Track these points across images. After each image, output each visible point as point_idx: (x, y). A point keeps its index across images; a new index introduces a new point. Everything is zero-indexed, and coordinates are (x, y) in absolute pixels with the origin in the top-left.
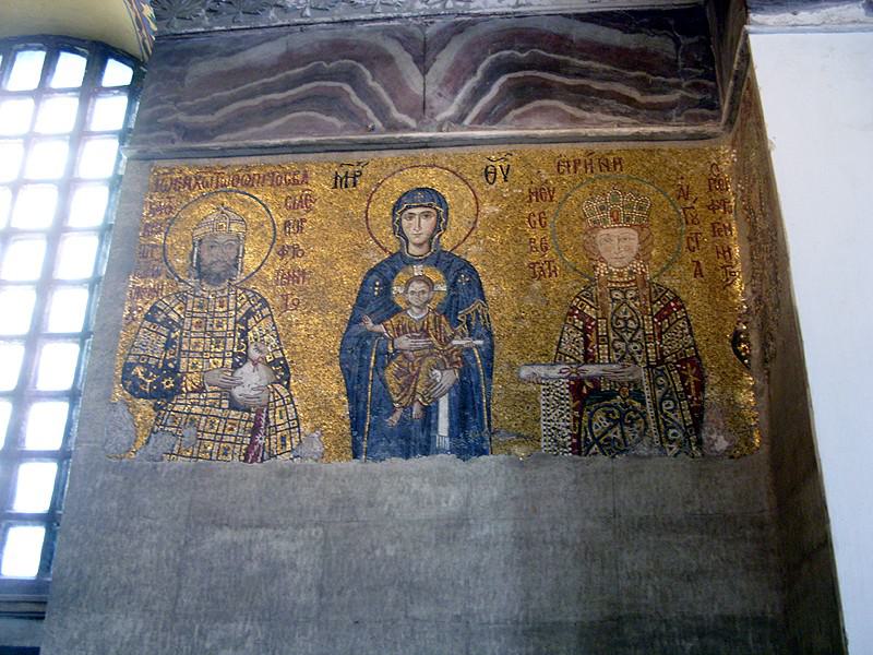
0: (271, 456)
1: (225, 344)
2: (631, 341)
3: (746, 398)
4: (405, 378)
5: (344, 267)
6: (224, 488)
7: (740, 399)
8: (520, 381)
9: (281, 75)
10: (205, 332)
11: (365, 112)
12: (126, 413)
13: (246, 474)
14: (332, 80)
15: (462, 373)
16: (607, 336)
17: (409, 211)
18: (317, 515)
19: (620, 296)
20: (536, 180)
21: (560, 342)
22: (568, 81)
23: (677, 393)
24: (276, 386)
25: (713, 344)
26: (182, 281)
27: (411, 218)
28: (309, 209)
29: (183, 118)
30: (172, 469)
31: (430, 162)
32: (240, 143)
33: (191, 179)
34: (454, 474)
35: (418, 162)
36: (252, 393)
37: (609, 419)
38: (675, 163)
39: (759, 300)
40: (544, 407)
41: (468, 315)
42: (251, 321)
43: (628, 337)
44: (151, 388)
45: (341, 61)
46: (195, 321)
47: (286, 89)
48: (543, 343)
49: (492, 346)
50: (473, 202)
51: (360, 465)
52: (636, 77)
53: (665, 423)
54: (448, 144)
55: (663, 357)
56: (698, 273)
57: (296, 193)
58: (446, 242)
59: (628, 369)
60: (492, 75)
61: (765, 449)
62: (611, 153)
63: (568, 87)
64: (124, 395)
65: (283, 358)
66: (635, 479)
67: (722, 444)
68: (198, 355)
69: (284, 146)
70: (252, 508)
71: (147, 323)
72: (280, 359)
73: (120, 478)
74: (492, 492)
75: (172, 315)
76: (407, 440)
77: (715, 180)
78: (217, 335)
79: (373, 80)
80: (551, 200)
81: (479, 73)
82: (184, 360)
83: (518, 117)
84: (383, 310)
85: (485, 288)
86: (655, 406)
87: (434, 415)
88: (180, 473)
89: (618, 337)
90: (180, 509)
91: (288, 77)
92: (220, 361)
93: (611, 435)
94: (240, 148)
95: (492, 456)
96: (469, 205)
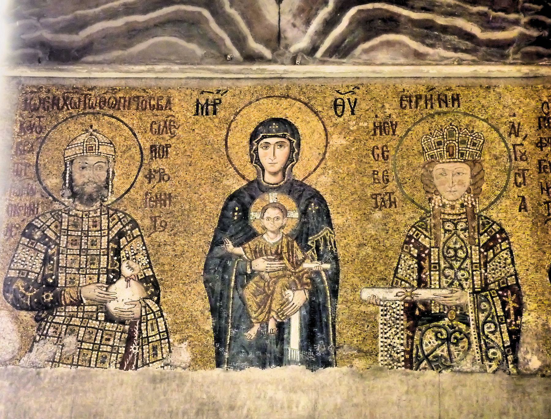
1: (100, 261)
2: (460, 269)
4: (261, 297)
5: (206, 191)
6: (103, 391)
8: (362, 302)
10: (80, 250)
12: (9, 324)
13: (122, 381)
15: (311, 294)
16: (439, 264)
17: (265, 140)
18: (186, 417)
20: (380, 115)
23: (498, 317)
27: (266, 147)
28: (173, 135)
29: (47, 35)
30: (54, 375)
31: (284, 92)
33: (59, 99)
34: (303, 382)
35: (274, 91)
36: (126, 307)
37: (437, 338)
40: (381, 326)
41: (317, 241)
42: (123, 240)
43: (457, 265)
44: (31, 301)
46: (70, 239)
47: (145, 12)
49: (337, 273)
52: (479, 14)
53: (486, 343)
55: (487, 285)
56: (523, 208)
57: (160, 118)
58: (298, 173)
59: (454, 295)
62: (450, 89)
64: (7, 307)
65: (154, 276)
66: (458, 391)
67: (535, 363)
68: (74, 271)
71: (25, 240)
73: (7, 384)
75: (49, 233)
77: (545, 118)
78: (91, 252)
79: (231, 6)
80: (394, 134)
84: (241, 234)
85: (332, 216)
86: (478, 327)
87: (286, 331)
88: (62, 378)
89: (447, 265)
90: (63, 412)
93: (438, 352)
95: (335, 368)
96: (319, 138)
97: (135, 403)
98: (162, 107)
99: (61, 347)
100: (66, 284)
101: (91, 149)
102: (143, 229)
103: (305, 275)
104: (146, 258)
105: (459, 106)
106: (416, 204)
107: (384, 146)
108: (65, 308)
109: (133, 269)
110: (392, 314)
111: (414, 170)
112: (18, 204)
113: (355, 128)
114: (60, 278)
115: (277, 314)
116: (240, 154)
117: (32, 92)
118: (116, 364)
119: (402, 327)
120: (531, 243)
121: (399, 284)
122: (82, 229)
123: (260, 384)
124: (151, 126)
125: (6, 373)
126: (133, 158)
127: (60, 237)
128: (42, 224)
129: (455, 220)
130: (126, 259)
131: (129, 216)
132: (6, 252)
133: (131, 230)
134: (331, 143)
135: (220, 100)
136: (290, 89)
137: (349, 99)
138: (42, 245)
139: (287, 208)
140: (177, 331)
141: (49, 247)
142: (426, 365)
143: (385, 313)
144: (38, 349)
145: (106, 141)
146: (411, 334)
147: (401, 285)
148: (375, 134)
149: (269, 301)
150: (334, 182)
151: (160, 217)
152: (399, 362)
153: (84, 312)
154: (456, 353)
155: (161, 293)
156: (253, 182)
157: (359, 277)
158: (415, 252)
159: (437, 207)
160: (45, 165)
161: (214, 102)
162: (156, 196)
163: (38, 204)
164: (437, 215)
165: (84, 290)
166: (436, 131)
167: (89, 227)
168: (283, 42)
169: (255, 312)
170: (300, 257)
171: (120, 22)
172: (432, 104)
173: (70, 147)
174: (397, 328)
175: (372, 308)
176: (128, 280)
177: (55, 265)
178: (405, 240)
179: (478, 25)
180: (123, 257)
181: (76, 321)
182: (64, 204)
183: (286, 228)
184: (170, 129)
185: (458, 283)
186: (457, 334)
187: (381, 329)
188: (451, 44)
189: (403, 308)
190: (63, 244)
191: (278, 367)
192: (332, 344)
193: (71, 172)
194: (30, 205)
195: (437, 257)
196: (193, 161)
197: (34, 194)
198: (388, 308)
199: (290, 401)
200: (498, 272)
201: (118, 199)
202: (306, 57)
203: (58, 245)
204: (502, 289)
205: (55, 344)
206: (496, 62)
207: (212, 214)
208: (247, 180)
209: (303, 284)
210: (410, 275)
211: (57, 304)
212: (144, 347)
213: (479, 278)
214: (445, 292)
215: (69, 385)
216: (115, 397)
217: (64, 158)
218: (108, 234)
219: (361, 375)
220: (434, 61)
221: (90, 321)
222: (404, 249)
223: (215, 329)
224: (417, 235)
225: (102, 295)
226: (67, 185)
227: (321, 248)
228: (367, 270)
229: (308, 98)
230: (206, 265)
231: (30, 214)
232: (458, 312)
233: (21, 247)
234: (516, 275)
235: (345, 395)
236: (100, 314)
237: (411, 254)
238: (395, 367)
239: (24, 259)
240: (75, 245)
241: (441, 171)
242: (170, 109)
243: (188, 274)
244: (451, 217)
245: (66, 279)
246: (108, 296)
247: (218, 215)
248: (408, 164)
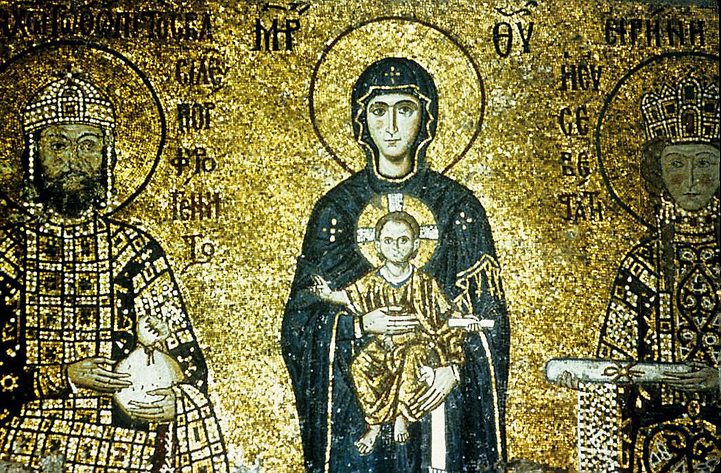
1: (97, 316)
2: (705, 329)
5: (280, 191)
8: (547, 383)
15: (463, 373)
16: (672, 321)
17: (378, 99)
21: (605, 326)
24: (185, 387)
36: (150, 399)
48: (581, 325)
50: (476, 86)
58: (437, 157)
62: (688, 12)
65: (195, 343)
72: (188, 345)
87: (425, 437)
92: (93, 346)
96: (470, 91)
100: (39, 359)
101: (70, 111)
102: (172, 259)
103: (453, 340)
104: (180, 310)
105: (702, 44)
107: (579, 109)
108: (41, 404)
109: (157, 331)
110: (599, 405)
114: (28, 348)
115: (408, 408)
119: (615, 428)
121: (609, 354)
122: (63, 257)
124: (178, 66)
126: (149, 129)
129: (696, 244)
130: (143, 312)
131: (148, 236)
133: (151, 260)
134: (490, 104)
135: (297, 22)
137: (519, 25)
139: (420, 223)
140: (239, 441)
143: (588, 402)
145: (98, 96)
148: (564, 87)
149: (394, 387)
150: (498, 175)
151: (200, 236)
153: (74, 409)
155: (211, 372)
157: (543, 342)
158: (634, 300)
159: (667, 222)
161: (288, 25)
162: (192, 198)
166: (666, 87)
167: (75, 256)
169: (374, 404)
170: (444, 307)
173: (33, 106)
175: (563, 395)
177: (19, 325)
178: (617, 278)
180: (139, 308)
181: (60, 426)
183: (418, 257)
184: (212, 77)
185: (702, 354)
186: (702, 440)
187: (582, 430)
189: (615, 395)
190: (31, 287)
193: (37, 154)
195: (669, 309)
198: (592, 394)
203: (23, 289)
207: (291, 232)
208: (350, 171)
209: (449, 356)
210: (626, 339)
214: (680, 368)
221: (87, 426)
222: (616, 294)
223: (304, 435)
224: (637, 268)
225: (109, 379)
226: (32, 178)
227: (478, 292)
228: (555, 327)
229: (449, 22)
232: (704, 404)
236: (103, 413)
240: (53, 288)
242: (210, 37)
243: (254, 339)
246: (115, 381)
247: (301, 233)
248: (619, 144)
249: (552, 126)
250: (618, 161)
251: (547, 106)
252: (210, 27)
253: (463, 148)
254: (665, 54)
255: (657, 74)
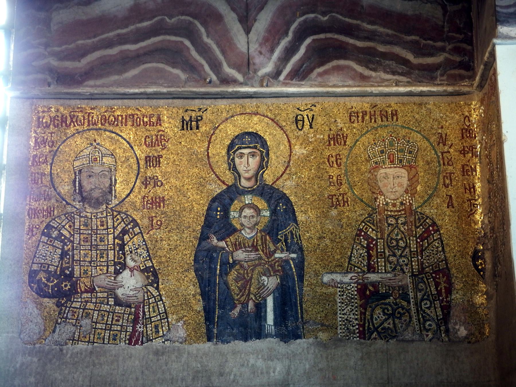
0: (149, 340)
1: (108, 255)
2: (401, 256)
3: (480, 299)
6: (116, 364)
7: (477, 301)
8: (323, 284)
9: (132, 27)
10: (91, 245)
11: (202, 66)
12: (35, 309)
13: (131, 354)
14: (176, 35)
16: (384, 252)
17: (240, 151)
18: (184, 383)
19: (393, 222)
20: (333, 128)
21: (351, 256)
22: (359, 44)
23: (432, 295)
25: (459, 259)
26: (70, 204)
28: (164, 148)
32: (106, 90)
35: (245, 109)
36: (131, 293)
37: (384, 314)
38: (437, 114)
39: (492, 229)
40: (339, 304)
41: (285, 235)
42: (126, 237)
43: (399, 253)
44: (52, 290)
45: (180, 17)
46: (82, 237)
47: (136, 42)
48: (339, 257)
51: (213, 347)
52: (412, 42)
53: (423, 317)
54: (269, 96)
55: (423, 269)
56: (450, 205)
58: (268, 177)
60: (299, 38)
61: (493, 337)
62: (390, 106)
63: (361, 50)
65: (153, 267)
66: (402, 356)
67: (463, 332)
68: (87, 264)
69: (141, 94)
70: (137, 379)
71: (44, 239)
73: (35, 359)
74: (304, 366)
75: (65, 232)
76: (245, 329)
77: (466, 130)
78: (101, 247)
79: (208, 36)
80: (345, 145)
81: (290, 34)
82: (77, 268)
83: (320, 75)
84: (223, 230)
85: (297, 214)
86: (416, 304)
87: (263, 310)
88: (81, 354)
89: (391, 253)
90: (83, 381)
91: (138, 30)
92: (105, 268)
93: (386, 325)
94: (105, 94)
95: (304, 340)
96: (284, 147)
97: (142, 372)
98: (153, 123)
99: (79, 327)
100: (80, 274)
106: (365, 203)
107: (337, 155)
108: (81, 295)
111: (362, 175)
112: (37, 208)
113: (313, 139)
114: (75, 270)
115: (255, 296)
116: (219, 163)
117: (43, 112)
118: (125, 341)
119: (356, 305)
120: (457, 234)
122: (92, 227)
123: (243, 355)
124: (145, 139)
125: (34, 351)
126: (131, 168)
127: (74, 235)
128: (58, 224)
129: (396, 216)
131: (131, 217)
132: (28, 249)
134: (294, 152)
136: (259, 107)
137: (307, 115)
138: (59, 243)
141: (65, 244)
142: (376, 335)
144: (60, 330)
146: (363, 311)
147: (354, 270)
151: (156, 217)
152: (354, 334)
154: (400, 325)
155: (160, 280)
156: (231, 186)
157: (320, 265)
159: (381, 205)
160: (57, 174)
161: (197, 118)
163: (54, 208)
164: (382, 212)
165: (95, 279)
167: (97, 227)
168: (251, 67)
170: (272, 248)
171: (114, 51)
172: (375, 118)
174: (352, 306)
175: (331, 290)
176: (132, 270)
179: (411, 51)
182: (75, 207)
183: (260, 224)
184: (161, 142)
186: (400, 310)
187: (340, 307)
188: (390, 68)
189: (356, 289)
190: (76, 242)
191: (258, 340)
192: (300, 320)
194: (47, 208)
195: (382, 247)
196: (182, 169)
197: (50, 199)
199: (268, 368)
200: (431, 259)
201: (120, 202)
202: (271, 79)
203: (73, 242)
204: (435, 272)
205: (74, 326)
206: (427, 83)
208: (227, 185)
209: (275, 271)
210: (361, 262)
211: (74, 291)
212: (148, 326)
213: (417, 263)
214: (389, 275)
215: (88, 359)
216: (125, 368)
217: (74, 168)
218: (114, 231)
219: (325, 344)
220: (376, 82)
221: (102, 305)
226: (77, 191)
227: (289, 241)
228: (326, 258)
230: (195, 256)
231: (48, 217)
232: (401, 292)
233: (41, 244)
234: (446, 260)
235: (312, 361)
236: (110, 299)
237: (361, 245)
238: (352, 338)
239: (45, 255)
240: (87, 241)
241: (384, 175)
242: (160, 125)
244: (393, 214)
245: (80, 270)
247: (203, 214)
248: (357, 169)
249: (324, 162)
250: (357, 177)
251: (321, 154)
252: (160, 120)
253: (281, 173)
254: (379, 127)
255: (375, 135)
